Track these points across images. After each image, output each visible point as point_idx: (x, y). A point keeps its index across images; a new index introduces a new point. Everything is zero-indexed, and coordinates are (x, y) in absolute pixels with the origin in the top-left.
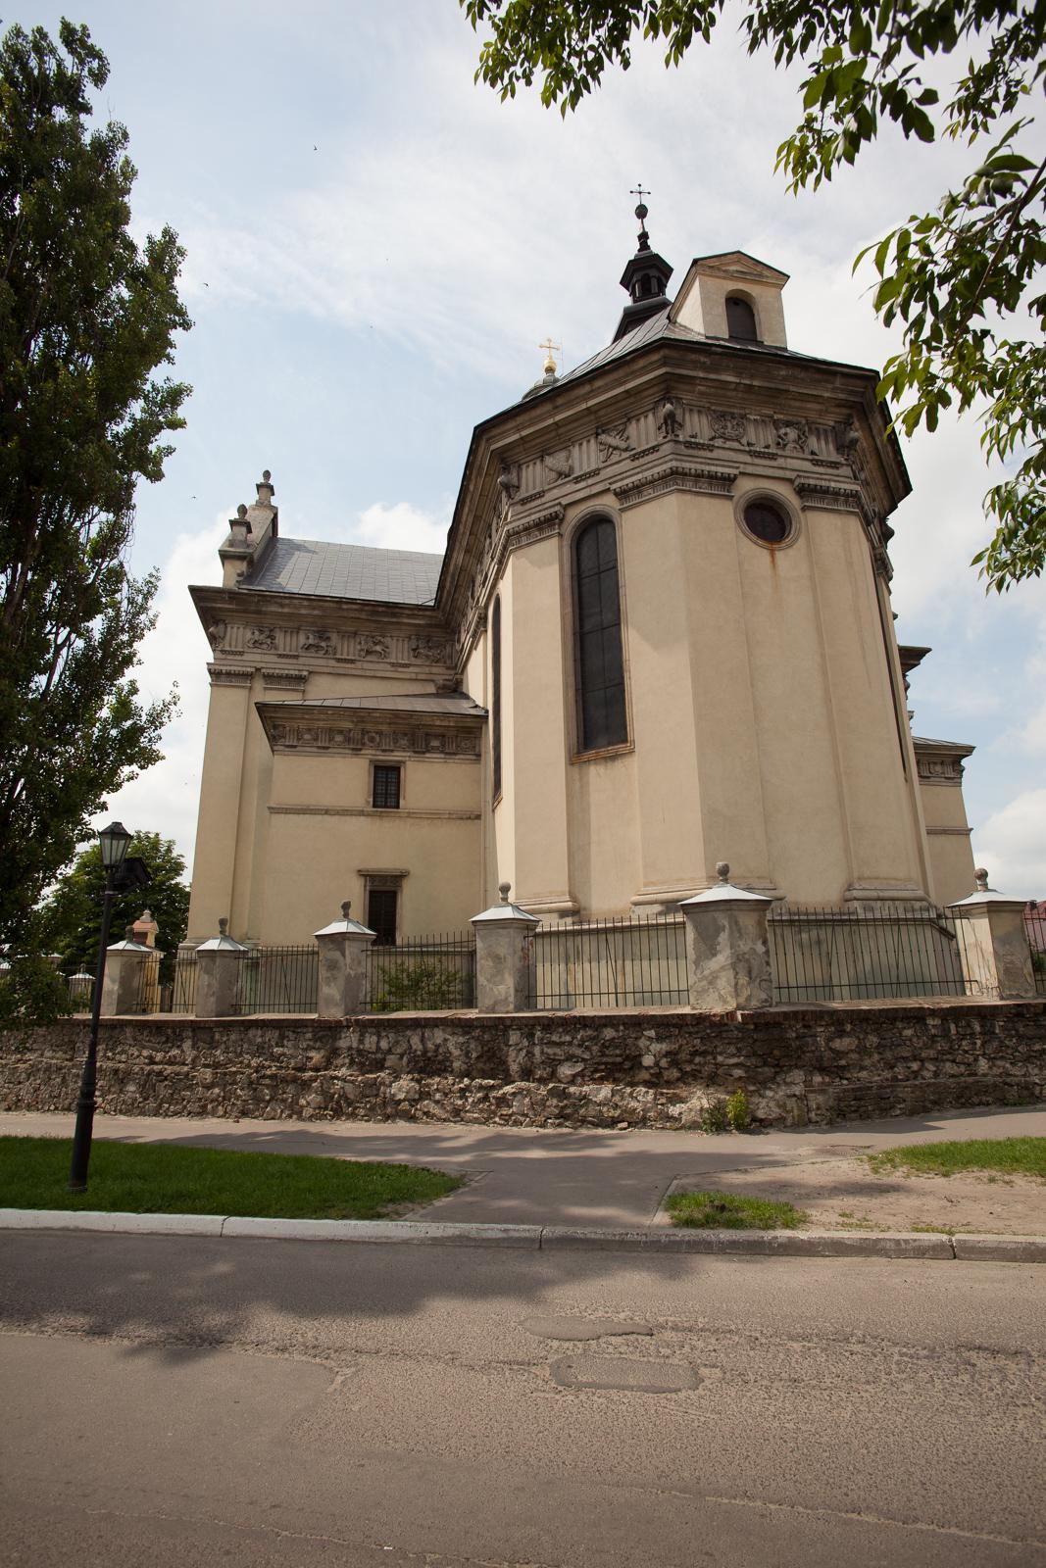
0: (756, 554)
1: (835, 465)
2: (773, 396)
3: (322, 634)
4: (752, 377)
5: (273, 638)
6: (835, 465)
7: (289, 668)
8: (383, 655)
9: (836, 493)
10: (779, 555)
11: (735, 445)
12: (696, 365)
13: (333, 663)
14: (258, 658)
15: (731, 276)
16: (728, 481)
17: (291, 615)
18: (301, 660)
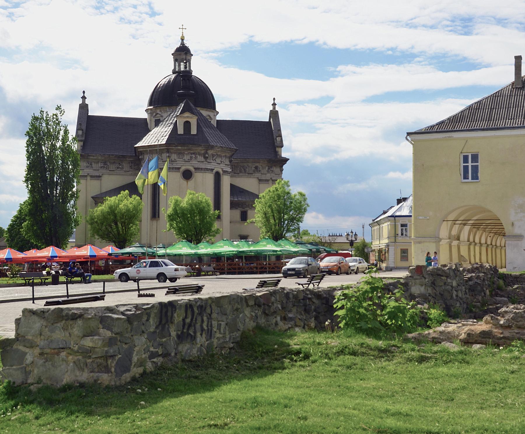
0: (184, 182)
1: (203, 162)
2: (189, 149)
3: (105, 163)
4: (184, 147)
5: (91, 164)
6: (203, 162)
7: (96, 173)
8: (122, 168)
9: (202, 168)
10: (189, 182)
11: (182, 160)
12: (172, 146)
13: (108, 171)
14: (88, 171)
15: (185, 117)
16: (179, 169)
17: (95, 159)
18: (100, 171)
